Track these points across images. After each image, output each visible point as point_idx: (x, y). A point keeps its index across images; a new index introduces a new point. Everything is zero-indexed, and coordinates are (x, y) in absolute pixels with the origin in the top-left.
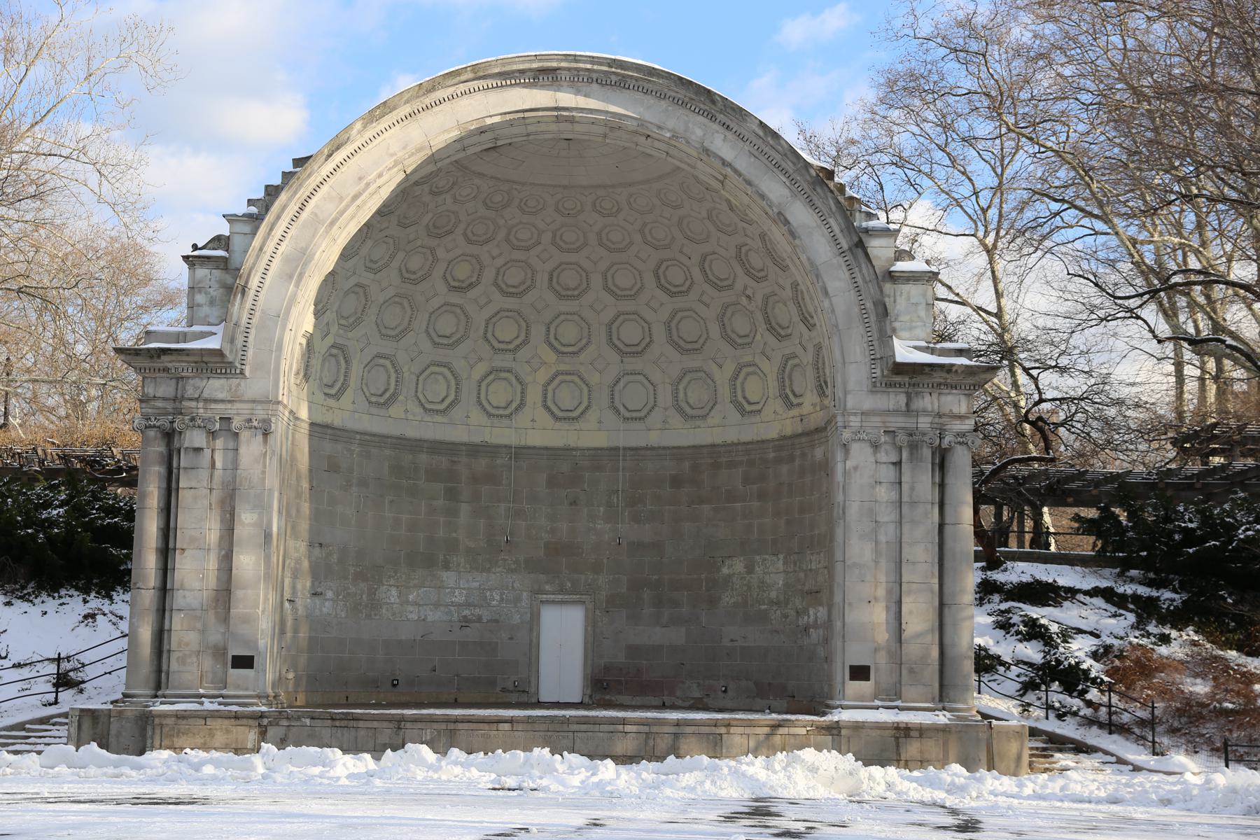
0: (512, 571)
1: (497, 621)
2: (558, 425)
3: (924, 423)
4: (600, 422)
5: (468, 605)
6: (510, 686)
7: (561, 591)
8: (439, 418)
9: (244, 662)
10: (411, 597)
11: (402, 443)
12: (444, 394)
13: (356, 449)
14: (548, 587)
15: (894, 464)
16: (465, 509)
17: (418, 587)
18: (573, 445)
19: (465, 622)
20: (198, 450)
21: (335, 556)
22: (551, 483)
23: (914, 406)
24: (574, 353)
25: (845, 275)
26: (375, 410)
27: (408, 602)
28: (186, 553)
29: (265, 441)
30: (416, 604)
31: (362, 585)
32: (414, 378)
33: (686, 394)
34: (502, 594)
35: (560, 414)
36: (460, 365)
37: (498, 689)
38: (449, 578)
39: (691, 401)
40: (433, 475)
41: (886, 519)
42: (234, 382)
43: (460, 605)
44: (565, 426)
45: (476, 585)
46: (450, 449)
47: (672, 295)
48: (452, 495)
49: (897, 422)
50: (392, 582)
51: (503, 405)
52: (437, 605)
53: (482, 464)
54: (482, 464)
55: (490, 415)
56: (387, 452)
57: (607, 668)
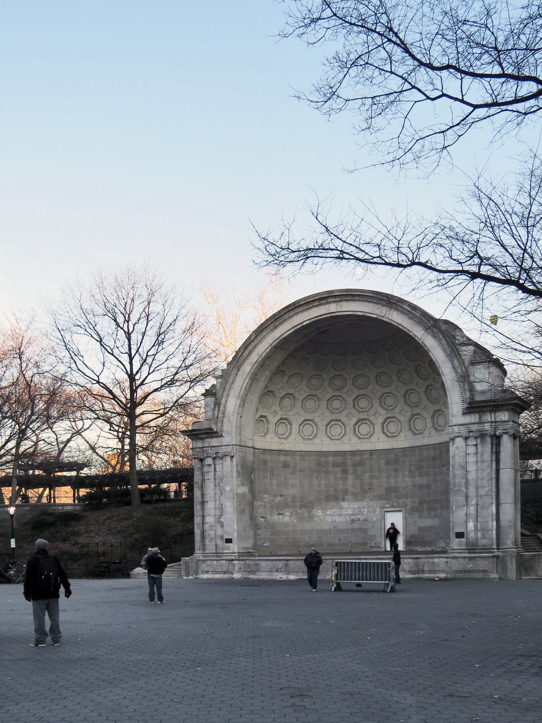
0: (372, 500)
1: (366, 520)
2: (389, 439)
3: (487, 427)
4: (405, 436)
5: (353, 514)
6: (373, 545)
7: (392, 506)
8: (337, 442)
9: (229, 541)
10: (328, 513)
11: (320, 454)
12: (340, 432)
13: (298, 458)
14: (387, 506)
15: (474, 445)
16: (351, 477)
17: (331, 509)
18: (395, 447)
19: (353, 521)
20: (210, 465)
21: (290, 499)
22: (387, 463)
23: (482, 420)
24: (392, 409)
25: (450, 365)
26: (305, 442)
27: (327, 515)
28: (209, 503)
29: (231, 460)
30: (330, 515)
31: (304, 510)
32: (325, 427)
33: (437, 421)
34: (368, 510)
35: (390, 435)
36: (344, 420)
37: (368, 546)
38: (345, 504)
39: (439, 424)
40: (335, 465)
41: (472, 469)
42: (220, 439)
43: (351, 515)
44: (391, 439)
45: (357, 506)
46: (343, 453)
47: (424, 380)
48: (345, 472)
49: (474, 428)
50: (319, 507)
51: (366, 433)
52: (340, 515)
53: (358, 458)
54: (358, 458)
55: (360, 438)
56: (314, 458)
57: (411, 536)
